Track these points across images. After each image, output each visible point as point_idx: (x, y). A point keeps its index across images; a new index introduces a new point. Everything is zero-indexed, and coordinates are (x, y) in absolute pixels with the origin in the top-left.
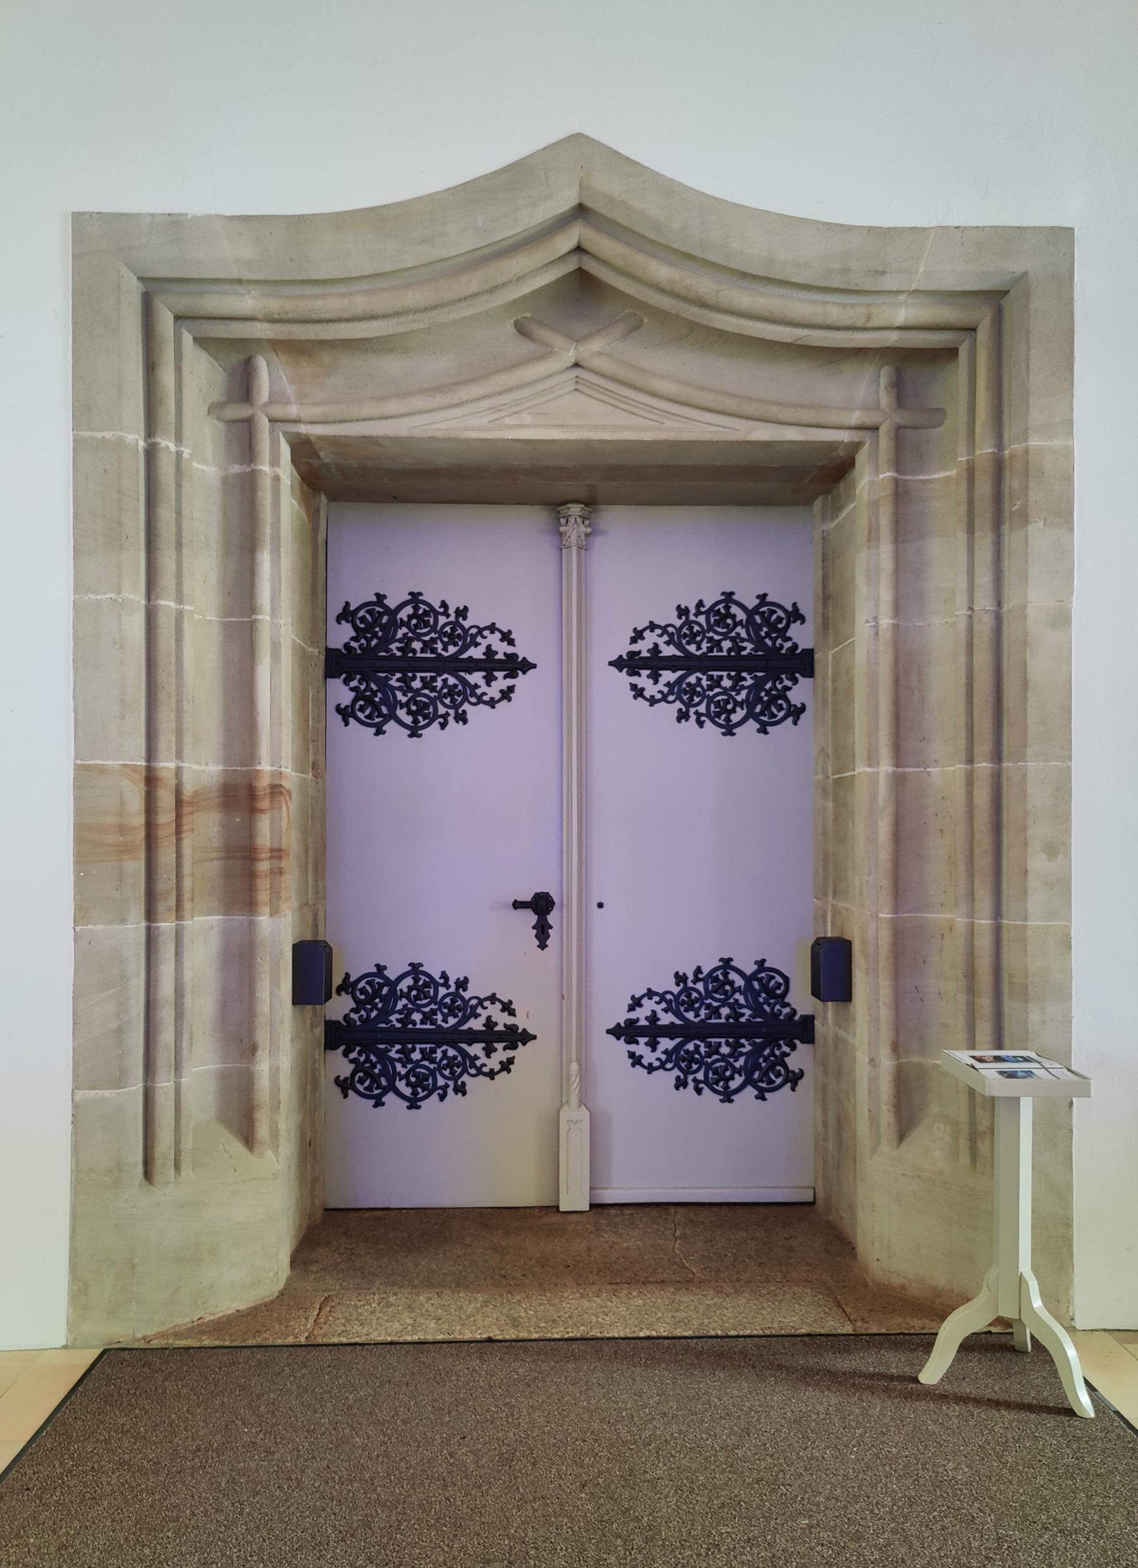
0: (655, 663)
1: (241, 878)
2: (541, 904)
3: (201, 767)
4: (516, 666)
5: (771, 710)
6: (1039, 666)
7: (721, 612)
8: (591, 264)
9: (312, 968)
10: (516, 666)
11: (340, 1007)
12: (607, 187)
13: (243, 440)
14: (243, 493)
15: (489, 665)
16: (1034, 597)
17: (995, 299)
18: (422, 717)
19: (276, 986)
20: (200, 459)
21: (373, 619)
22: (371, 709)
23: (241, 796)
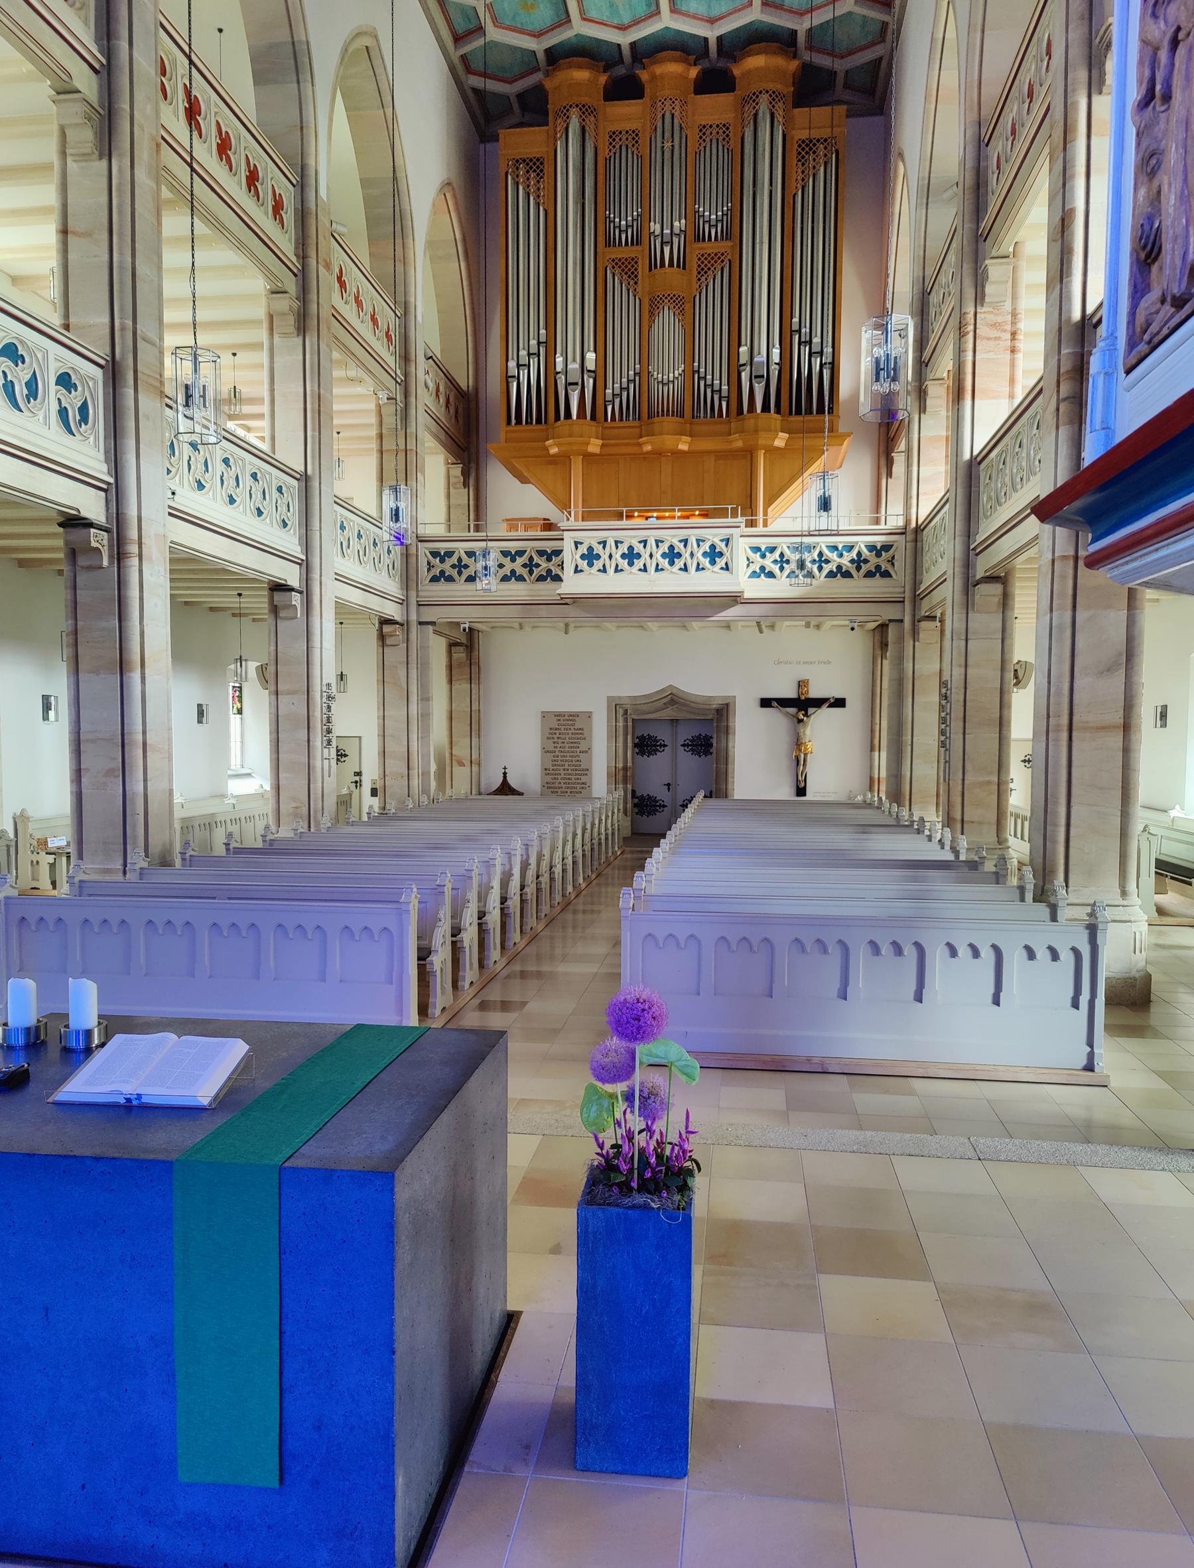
0: (688, 745)
1: (625, 782)
2: (669, 785)
3: (620, 765)
4: (665, 746)
5: (707, 752)
6: (730, 753)
7: (699, 737)
8: (673, 698)
9: (633, 792)
10: (665, 746)
11: (636, 801)
12: (675, 692)
13: (626, 720)
14: (626, 727)
15: (661, 746)
16: (730, 745)
17: (727, 705)
18: (650, 754)
19: (629, 796)
20: (621, 724)
21: (642, 738)
22: (642, 753)
23: (625, 769)
